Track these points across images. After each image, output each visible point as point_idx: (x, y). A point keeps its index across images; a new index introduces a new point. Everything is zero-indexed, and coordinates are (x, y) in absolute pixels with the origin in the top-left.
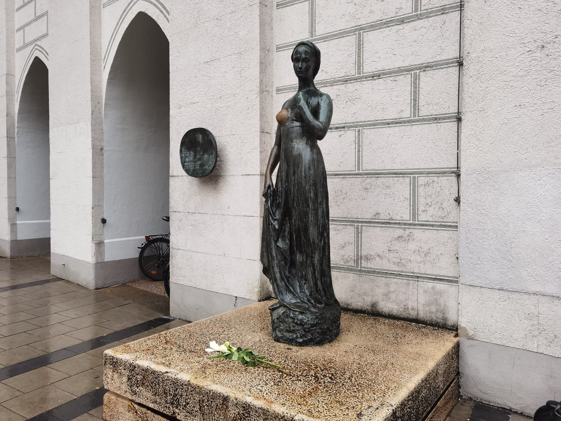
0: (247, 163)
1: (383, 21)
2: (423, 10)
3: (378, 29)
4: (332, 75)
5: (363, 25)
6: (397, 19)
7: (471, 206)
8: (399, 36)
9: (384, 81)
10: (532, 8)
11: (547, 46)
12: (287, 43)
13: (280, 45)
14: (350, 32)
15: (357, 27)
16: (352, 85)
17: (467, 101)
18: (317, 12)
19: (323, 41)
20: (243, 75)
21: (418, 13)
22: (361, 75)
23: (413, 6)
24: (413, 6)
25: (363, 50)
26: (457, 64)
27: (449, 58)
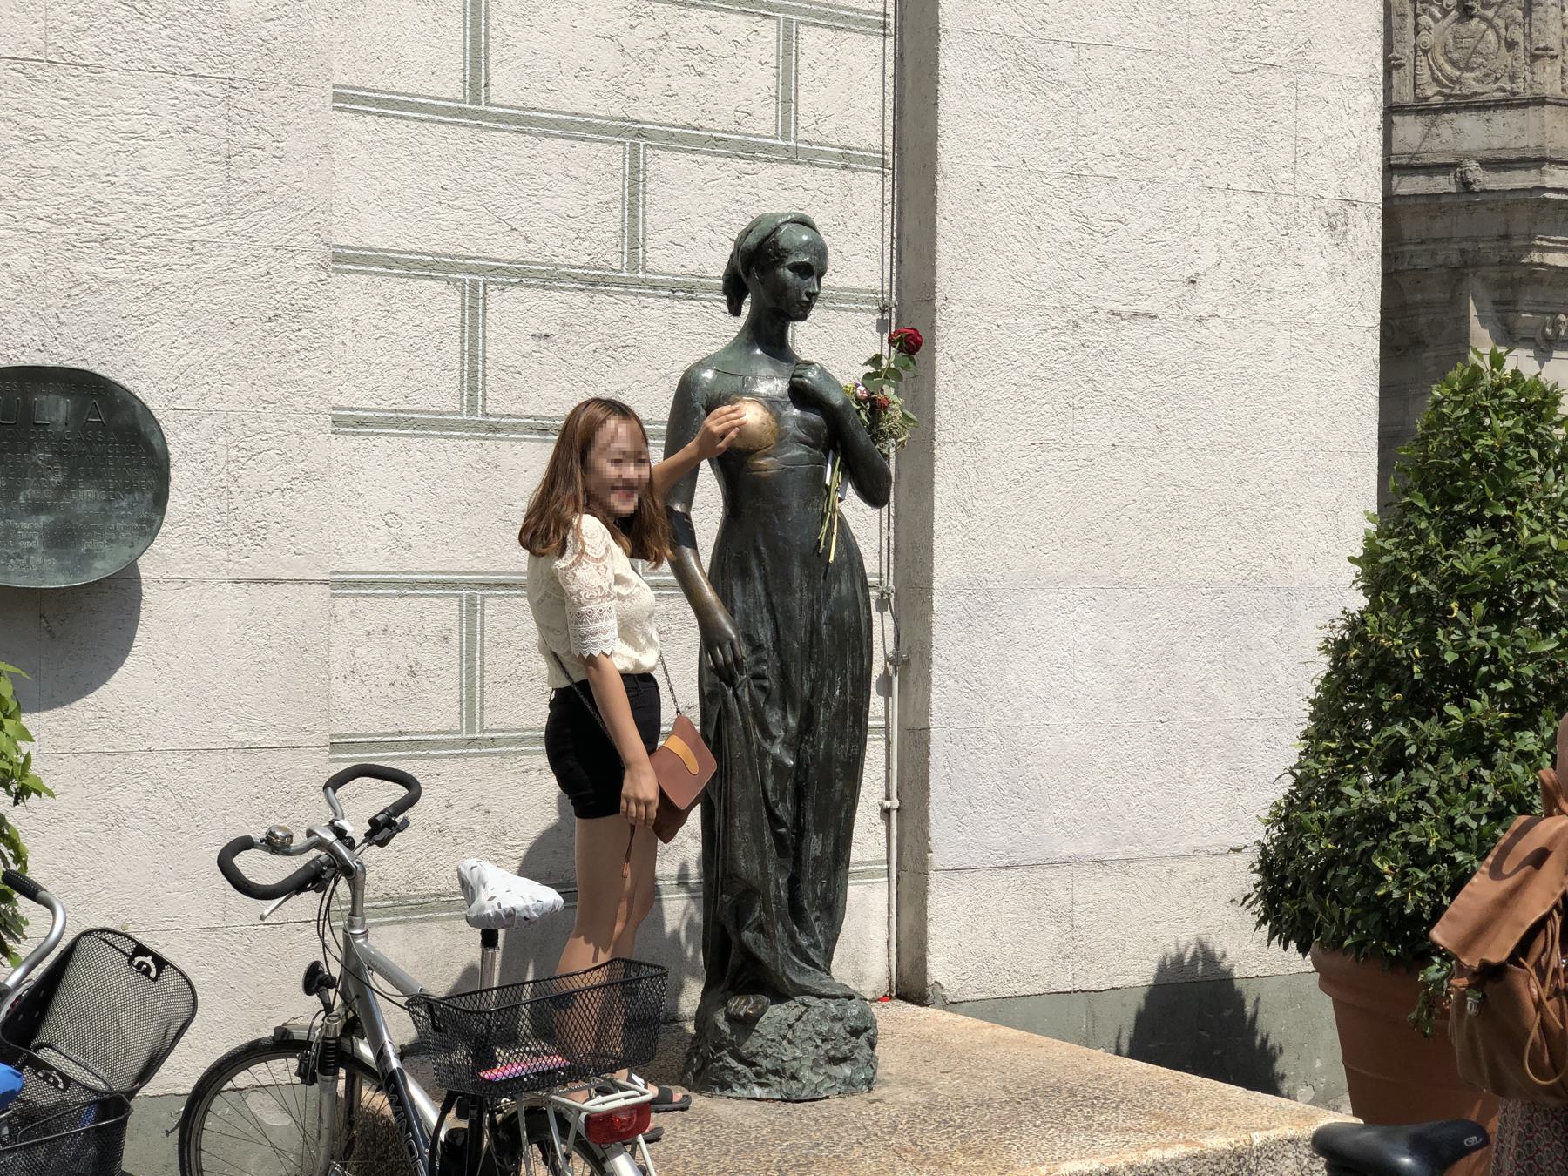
0: (264, 531)
1: (701, 133)
2: (802, 142)
3: (687, 151)
4: (549, 253)
5: (646, 123)
6: (740, 142)
7: (953, 673)
8: (744, 190)
9: (703, 309)
10: (1059, 236)
11: (1082, 324)
12: (374, 91)
13: (344, 87)
14: (602, 130)
15: (628, 124)
16: (612, 299)
17: (944, 414)
18: (493, 22)
19: (514, 127)
20: (245, 174)
21: (790, 144)
22: (640, 275)
23: (777, 121)
24: (777, 121)
25: (644, 199)
26: (876, 307)
27: (859, 287)
